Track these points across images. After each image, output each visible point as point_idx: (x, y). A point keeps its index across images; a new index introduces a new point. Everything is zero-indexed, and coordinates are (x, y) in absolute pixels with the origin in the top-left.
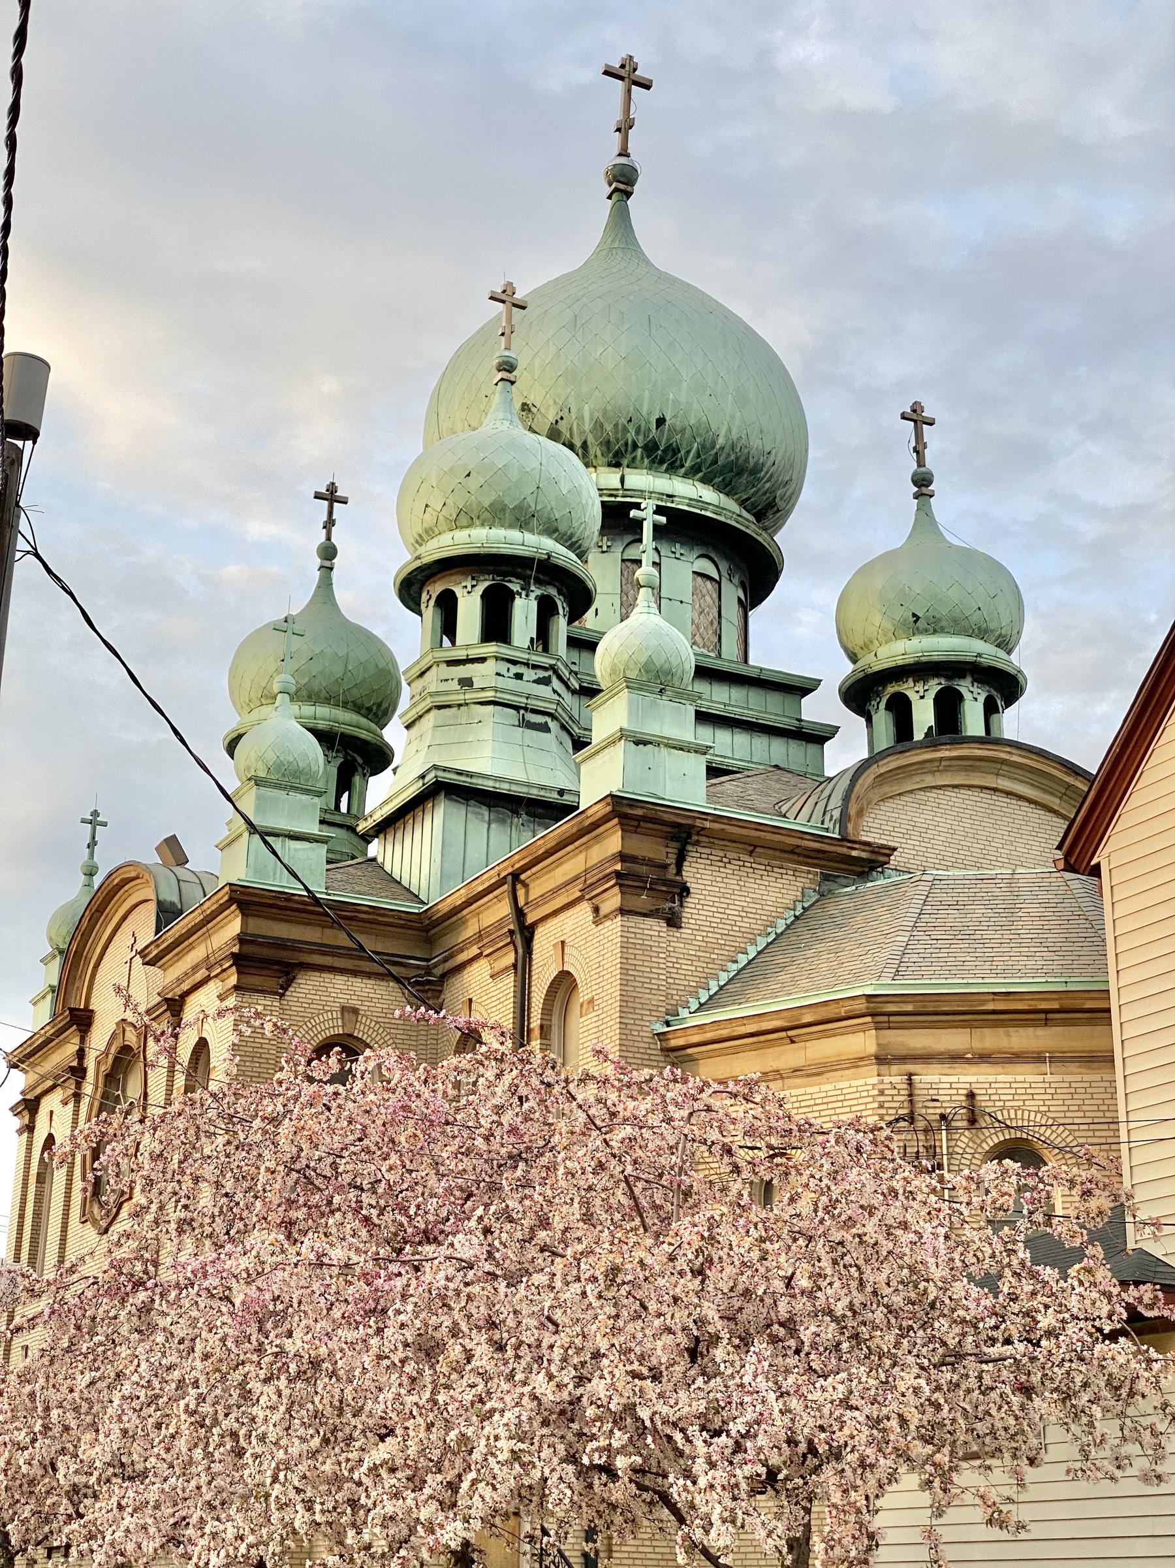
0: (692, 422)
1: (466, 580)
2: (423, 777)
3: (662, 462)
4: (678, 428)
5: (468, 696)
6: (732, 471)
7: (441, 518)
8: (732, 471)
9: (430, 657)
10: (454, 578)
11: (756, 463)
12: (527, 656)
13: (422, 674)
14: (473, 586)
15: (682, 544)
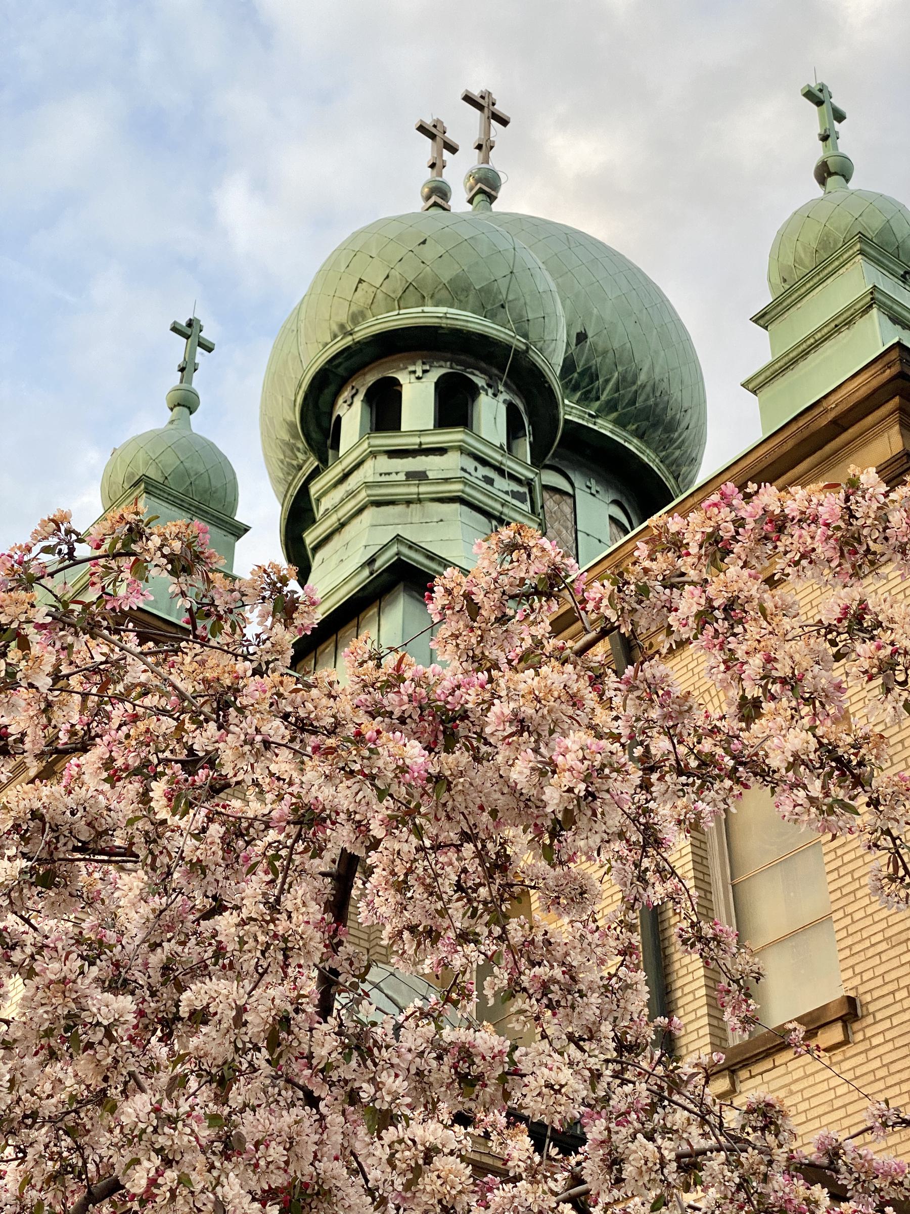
0: (616, 345)
1: (414, 364)
2: (371, 561)
3: (575, 389)
4: (600, 349)
5: (422, 489)
6: (647, 419)
7: (380, 296)
8: (647, 419)
9: (365, 445)
10: (395, 364)
11: (673, 418)
12: (499, 458)
13: (346, 476)
14: (425, 372)
15: (597, 482)
